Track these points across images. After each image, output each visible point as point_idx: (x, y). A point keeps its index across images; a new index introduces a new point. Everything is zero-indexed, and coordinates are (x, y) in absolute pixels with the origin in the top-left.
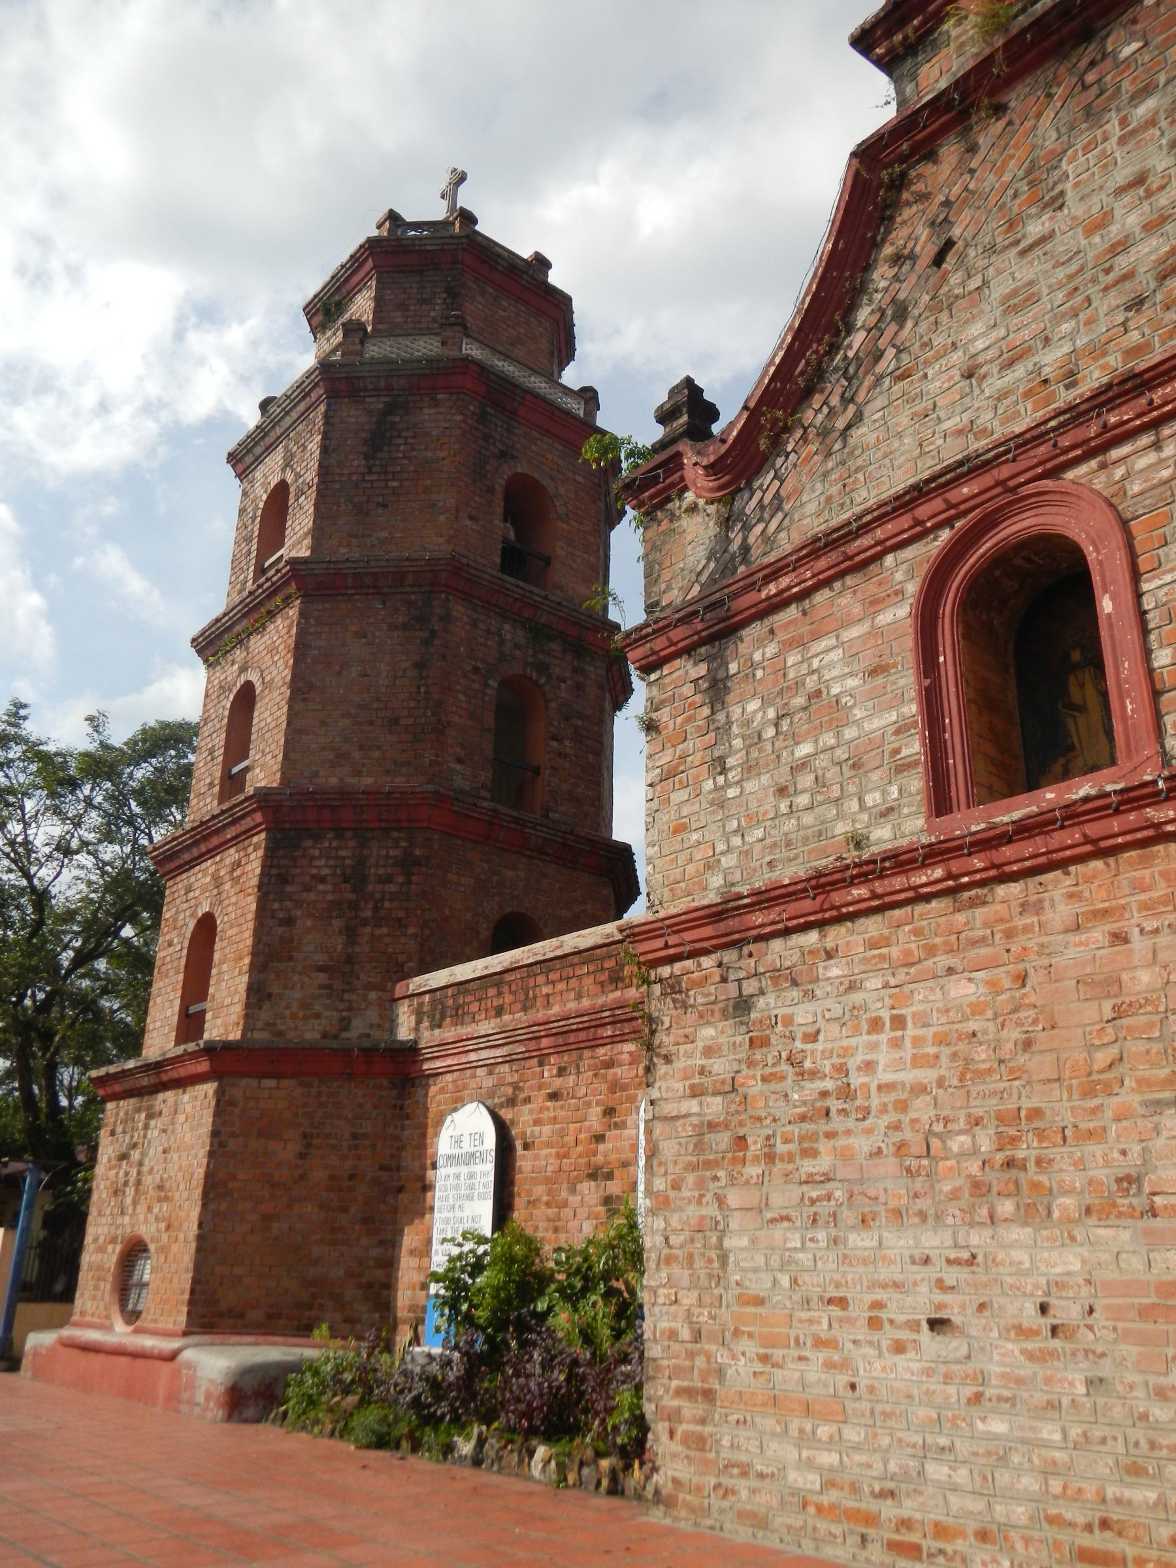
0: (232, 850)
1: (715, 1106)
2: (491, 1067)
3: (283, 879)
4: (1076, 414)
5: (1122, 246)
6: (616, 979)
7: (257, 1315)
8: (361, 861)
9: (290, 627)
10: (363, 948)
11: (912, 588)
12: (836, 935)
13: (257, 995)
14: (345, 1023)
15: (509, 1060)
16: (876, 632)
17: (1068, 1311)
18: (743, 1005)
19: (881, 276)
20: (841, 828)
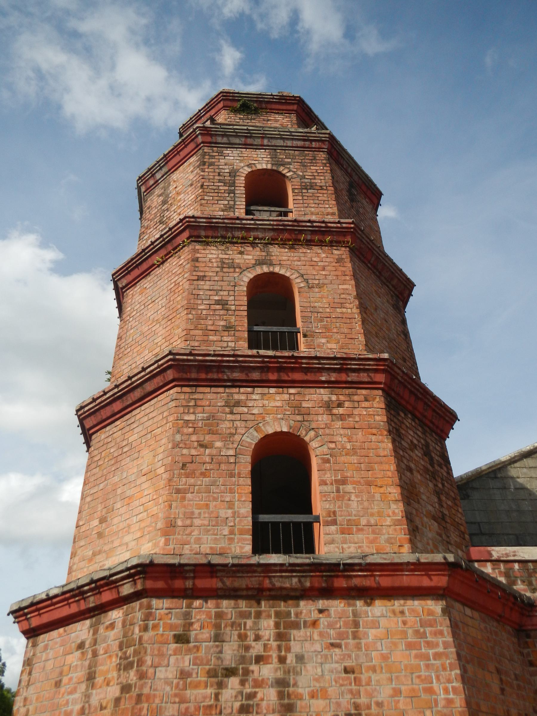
0: (322, 391)
9: (339, 260)
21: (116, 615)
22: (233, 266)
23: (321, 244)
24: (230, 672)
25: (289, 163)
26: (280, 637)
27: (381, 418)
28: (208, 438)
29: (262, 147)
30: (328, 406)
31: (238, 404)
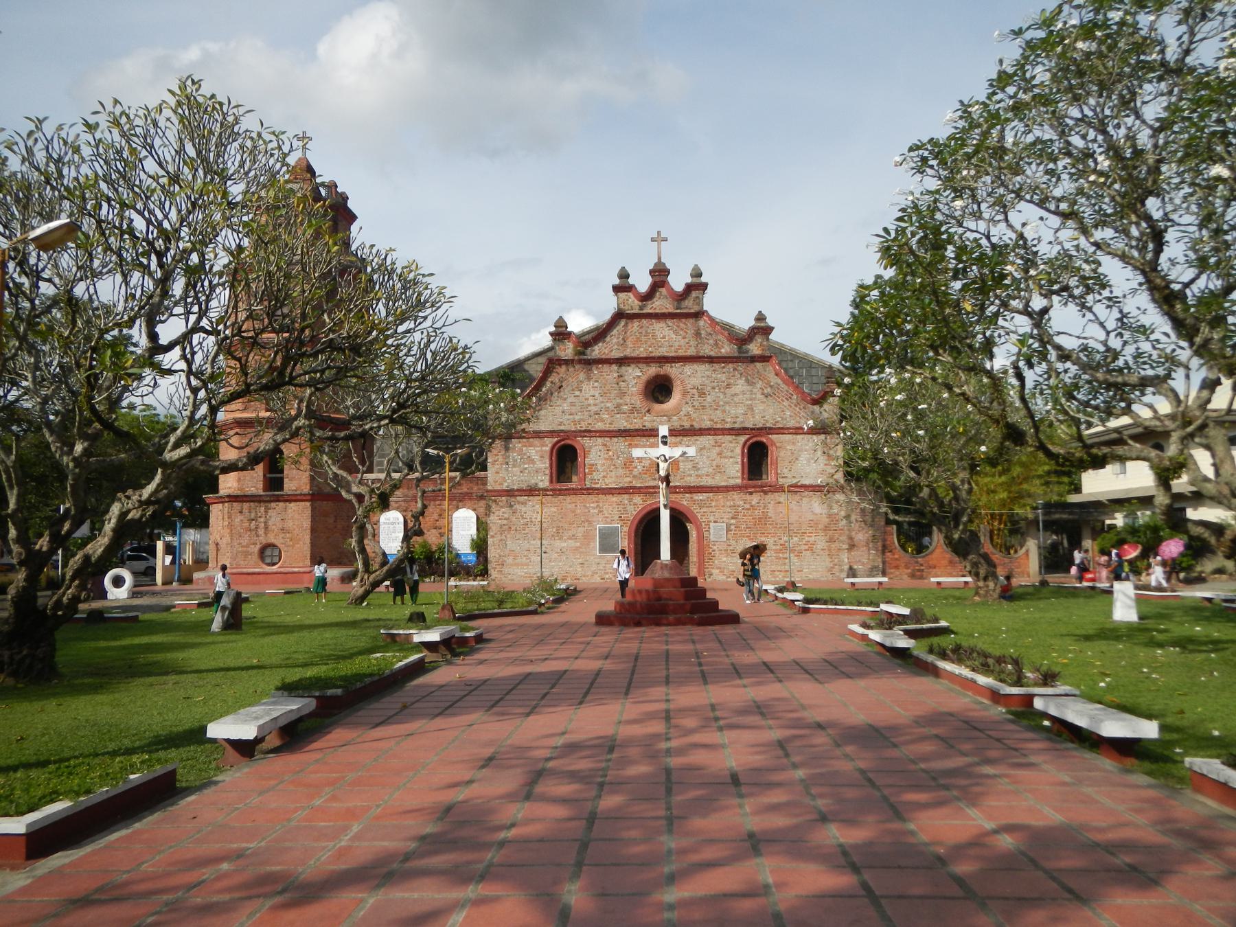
1: (505, 522)
4: (581, 431)
5: (589, 405)
11: (550, 445)
12: (531, 498)
15: (404, 501)
16: (542, 451)
17: (564, 550)
18: (511, 506)
19: (548, 384)
20: (533, 481)
26: (266, 512)
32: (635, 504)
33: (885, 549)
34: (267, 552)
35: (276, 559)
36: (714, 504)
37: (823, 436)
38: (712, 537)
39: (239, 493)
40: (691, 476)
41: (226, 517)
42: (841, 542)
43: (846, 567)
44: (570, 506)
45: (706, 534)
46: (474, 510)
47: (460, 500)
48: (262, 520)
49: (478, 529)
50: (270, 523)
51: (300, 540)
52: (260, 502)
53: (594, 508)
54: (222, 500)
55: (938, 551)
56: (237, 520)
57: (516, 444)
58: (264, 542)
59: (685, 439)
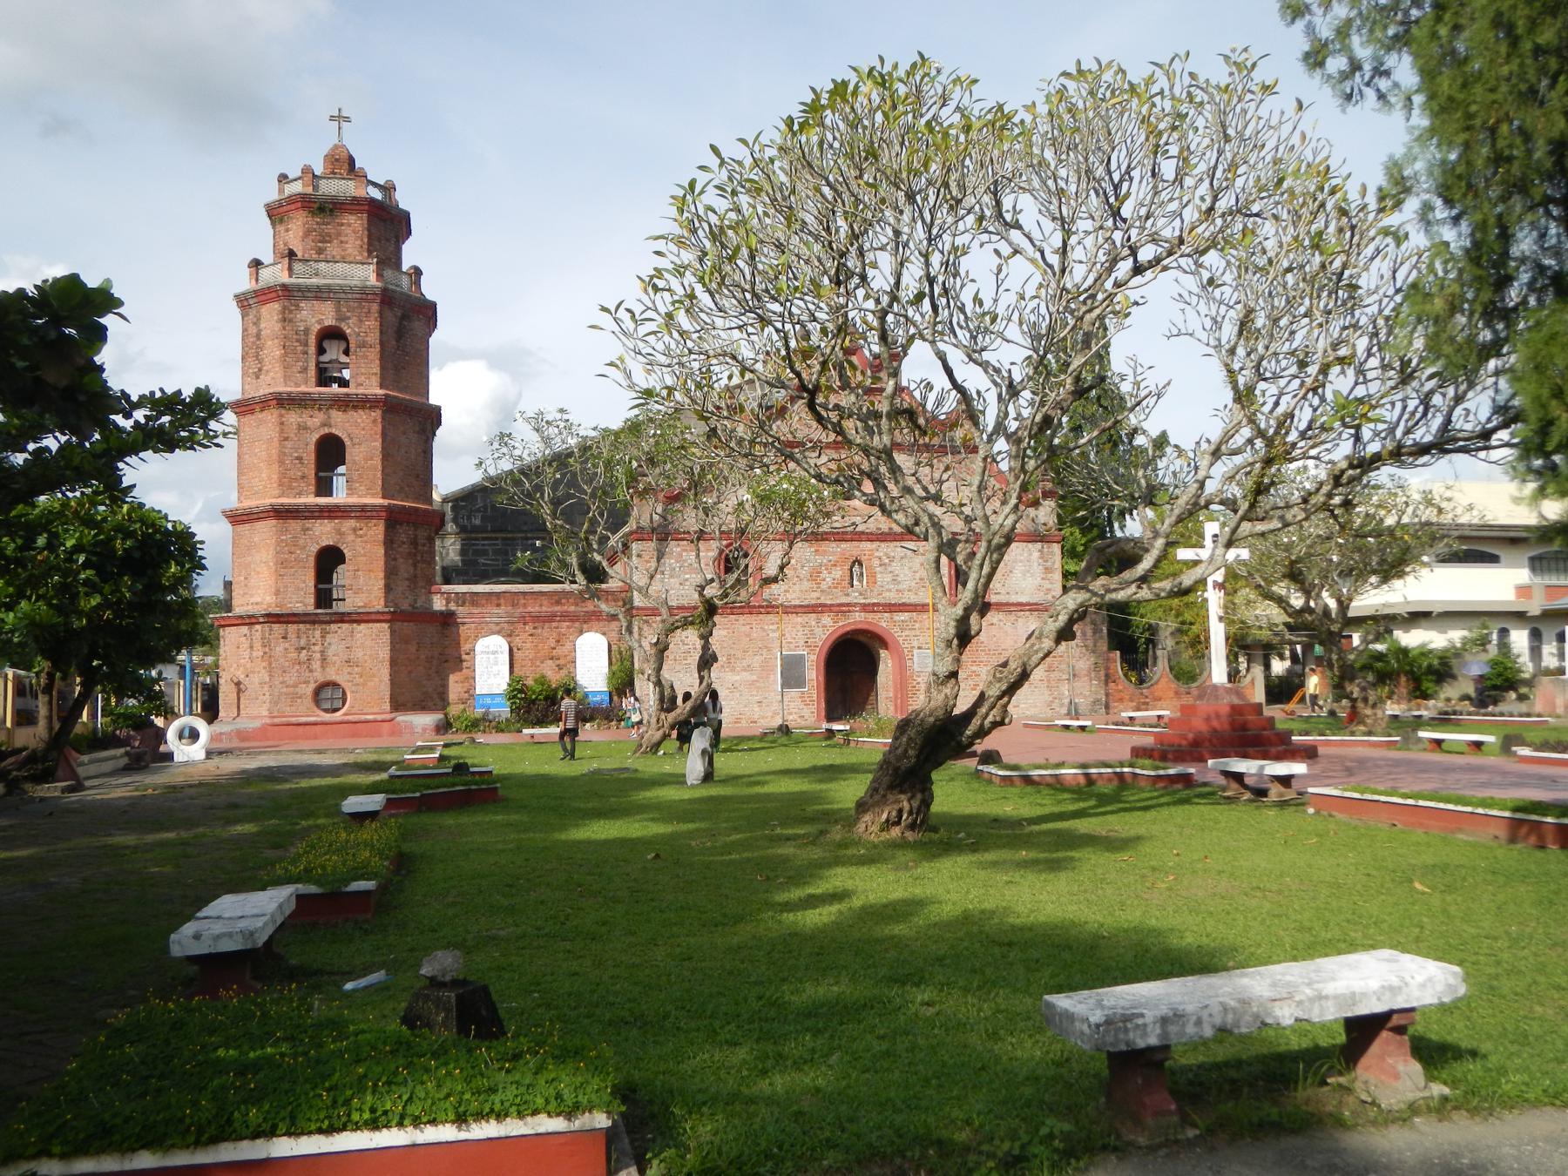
2: (497, 624)
3: (392, 542)
6: (558, 603)
7: (410, 705)
8: (416, 536)
9: (375, 421)
10: (419, 572)
13: (388, 588)
14: (416, 602)
17: (737, 685)
21: (258, 627)
22: (306, 428)
23: (363, 408)
24: (303, 648)
25: (349, 318)
27: (381, 537)
28: (293, 549)
29: (329, 299)
30: (354, 530)
31: (308, 529)
32: (824, 626)
33: (1108, 678)
34: (327, 693)
35: (338, 704)
36: (917, 625)
37: (1039, 545)
38: (916, 666)
39: (277, 611)
40: (890, 591)
41: (258, 645)
42: (1061, 671)
43: (1066, 701)
44: (743, 628)
45: (909, 663)
46: (604, 634)
47: (587, 620)
48: (317, 648)
49: (610, 663)
50: (330, 653)
51: (374, 676)
52: (313, 623)
53: (774, 631)
54: (249, 620)
55: (1164, 681)
56: (279, 649)
57: (674, 547)
58: (321, 679)
59: (883, 545)
